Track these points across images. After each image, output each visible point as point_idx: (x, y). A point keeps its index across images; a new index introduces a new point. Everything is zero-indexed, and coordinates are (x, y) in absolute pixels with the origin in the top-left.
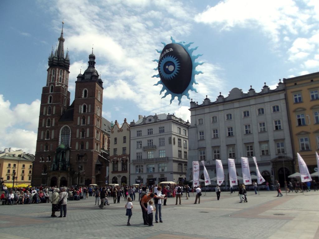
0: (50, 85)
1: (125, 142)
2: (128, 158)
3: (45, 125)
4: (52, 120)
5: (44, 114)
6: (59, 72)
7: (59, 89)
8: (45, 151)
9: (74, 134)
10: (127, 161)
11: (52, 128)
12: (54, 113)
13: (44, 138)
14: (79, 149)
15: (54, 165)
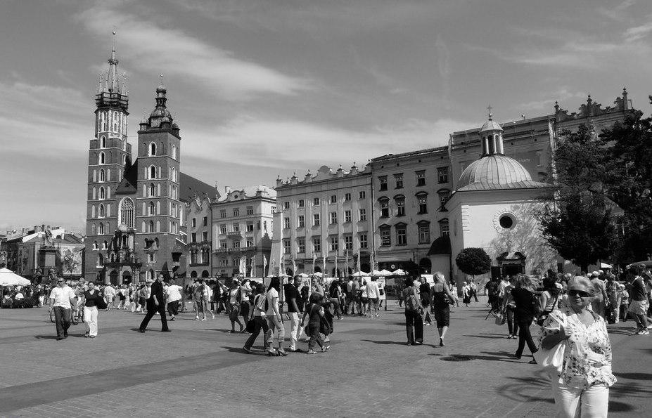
0: (100, 137)
1: (205, 225)
2: (210, 247)
3: (97, 197)
4: (107, 189)
5: (95, 180)
6: (112, 116)
7: (114, 143)
8: (99, 234)
9: (139, 210)
10: (208, 250)
11: (107, 202)
12: (109, 179)
13: (96, 216)
14: (147, 231)
15: (113, 255)
